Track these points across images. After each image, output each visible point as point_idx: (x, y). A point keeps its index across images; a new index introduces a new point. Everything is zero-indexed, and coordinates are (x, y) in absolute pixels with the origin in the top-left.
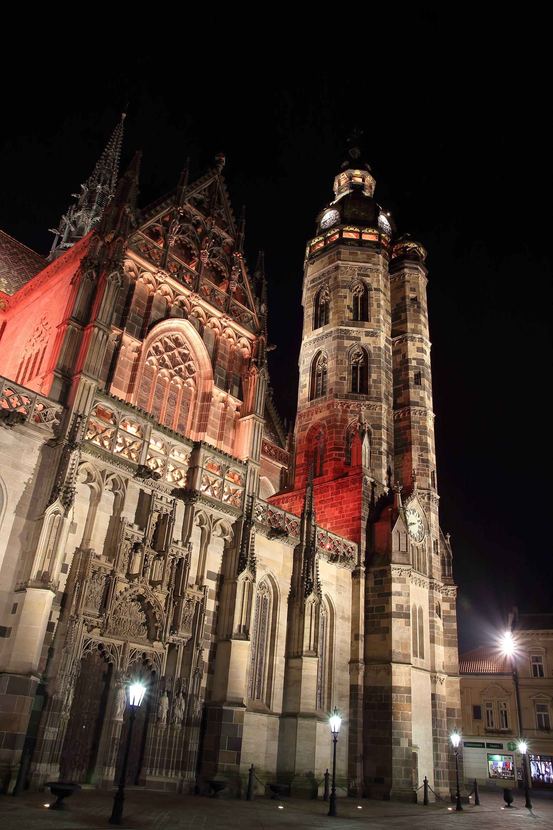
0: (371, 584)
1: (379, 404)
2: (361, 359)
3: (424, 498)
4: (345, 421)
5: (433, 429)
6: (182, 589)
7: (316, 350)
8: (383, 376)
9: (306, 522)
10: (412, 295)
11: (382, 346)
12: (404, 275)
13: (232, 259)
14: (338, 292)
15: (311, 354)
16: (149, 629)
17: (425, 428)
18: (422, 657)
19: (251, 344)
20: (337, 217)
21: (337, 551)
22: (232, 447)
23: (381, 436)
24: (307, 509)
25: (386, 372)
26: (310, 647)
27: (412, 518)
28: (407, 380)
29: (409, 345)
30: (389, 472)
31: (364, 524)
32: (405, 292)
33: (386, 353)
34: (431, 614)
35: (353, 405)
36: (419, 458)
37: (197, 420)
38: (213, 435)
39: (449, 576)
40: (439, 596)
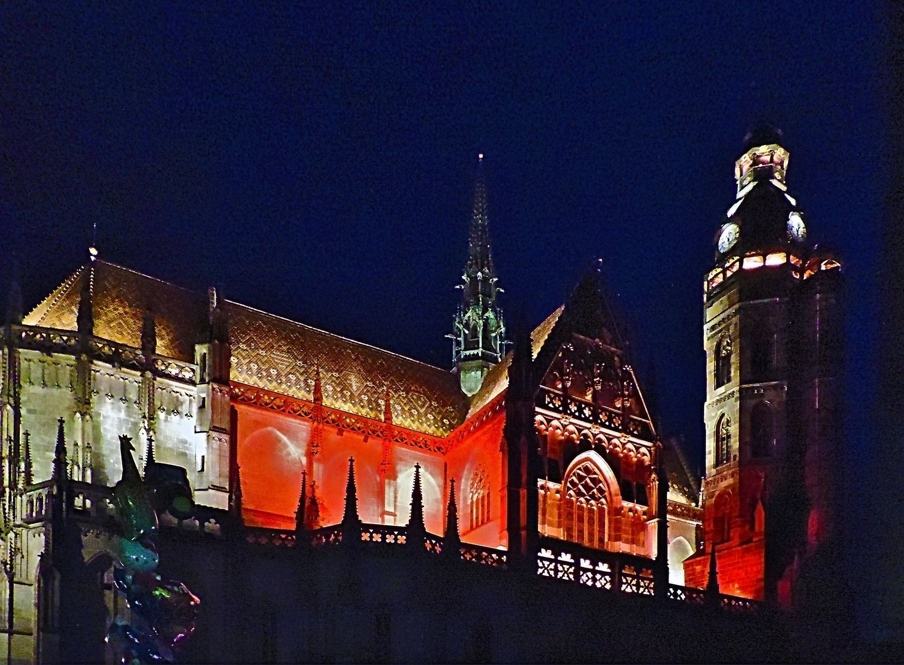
7: (719, 413)
15: (714, 417)
38: (627, 542)
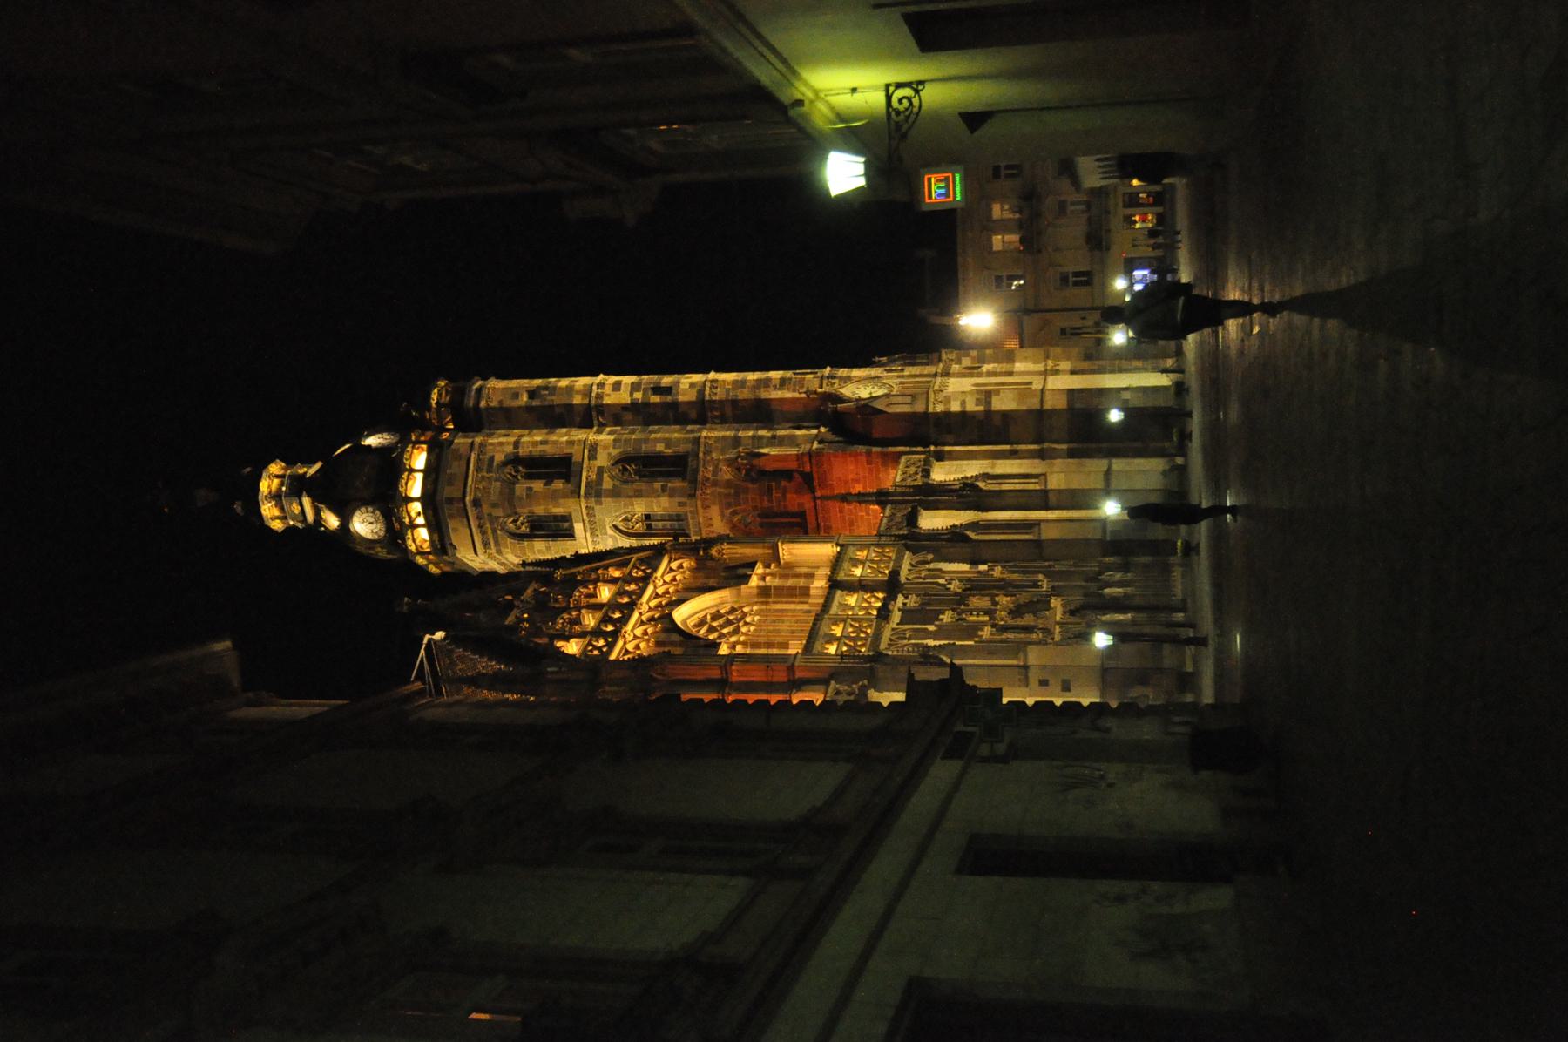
0: (950, 438)
1: (702, 440)
2: (631, 468)
3: (834, 384)
4: (728, 484)
5: (735, 374)
6: (996, 581)
7: (610, 532)
8: (659, 435)
9: (891, 498)
10: (525, 398)
11: (612, 437)
12: (488, 408)
13: (562, 582)
14: (521, 499)
16: (1041, 611)
17: (735, 382)
18: (1031, 383)
19: (675, 560)
20: (370, 509)
21: (916, 473)
22: (818, 567)
23: (749, 436)
24: (874, 499)
25: (651, 432)
26: (1035, 483)
27: (864, 393)
28: (663, 405)
29: (609, 402)
30: (799, 428)
31: (875, 449)
32: (520, 407)
33: (620, 434)
34: (980, 375)
35: (706, 472)
36: (779, 389)
37: (794, 600)
39: (928, 358)
40: (955, 368)
